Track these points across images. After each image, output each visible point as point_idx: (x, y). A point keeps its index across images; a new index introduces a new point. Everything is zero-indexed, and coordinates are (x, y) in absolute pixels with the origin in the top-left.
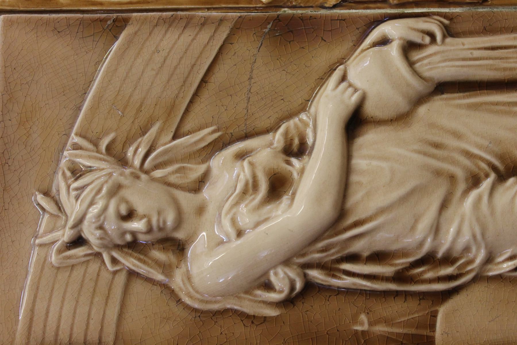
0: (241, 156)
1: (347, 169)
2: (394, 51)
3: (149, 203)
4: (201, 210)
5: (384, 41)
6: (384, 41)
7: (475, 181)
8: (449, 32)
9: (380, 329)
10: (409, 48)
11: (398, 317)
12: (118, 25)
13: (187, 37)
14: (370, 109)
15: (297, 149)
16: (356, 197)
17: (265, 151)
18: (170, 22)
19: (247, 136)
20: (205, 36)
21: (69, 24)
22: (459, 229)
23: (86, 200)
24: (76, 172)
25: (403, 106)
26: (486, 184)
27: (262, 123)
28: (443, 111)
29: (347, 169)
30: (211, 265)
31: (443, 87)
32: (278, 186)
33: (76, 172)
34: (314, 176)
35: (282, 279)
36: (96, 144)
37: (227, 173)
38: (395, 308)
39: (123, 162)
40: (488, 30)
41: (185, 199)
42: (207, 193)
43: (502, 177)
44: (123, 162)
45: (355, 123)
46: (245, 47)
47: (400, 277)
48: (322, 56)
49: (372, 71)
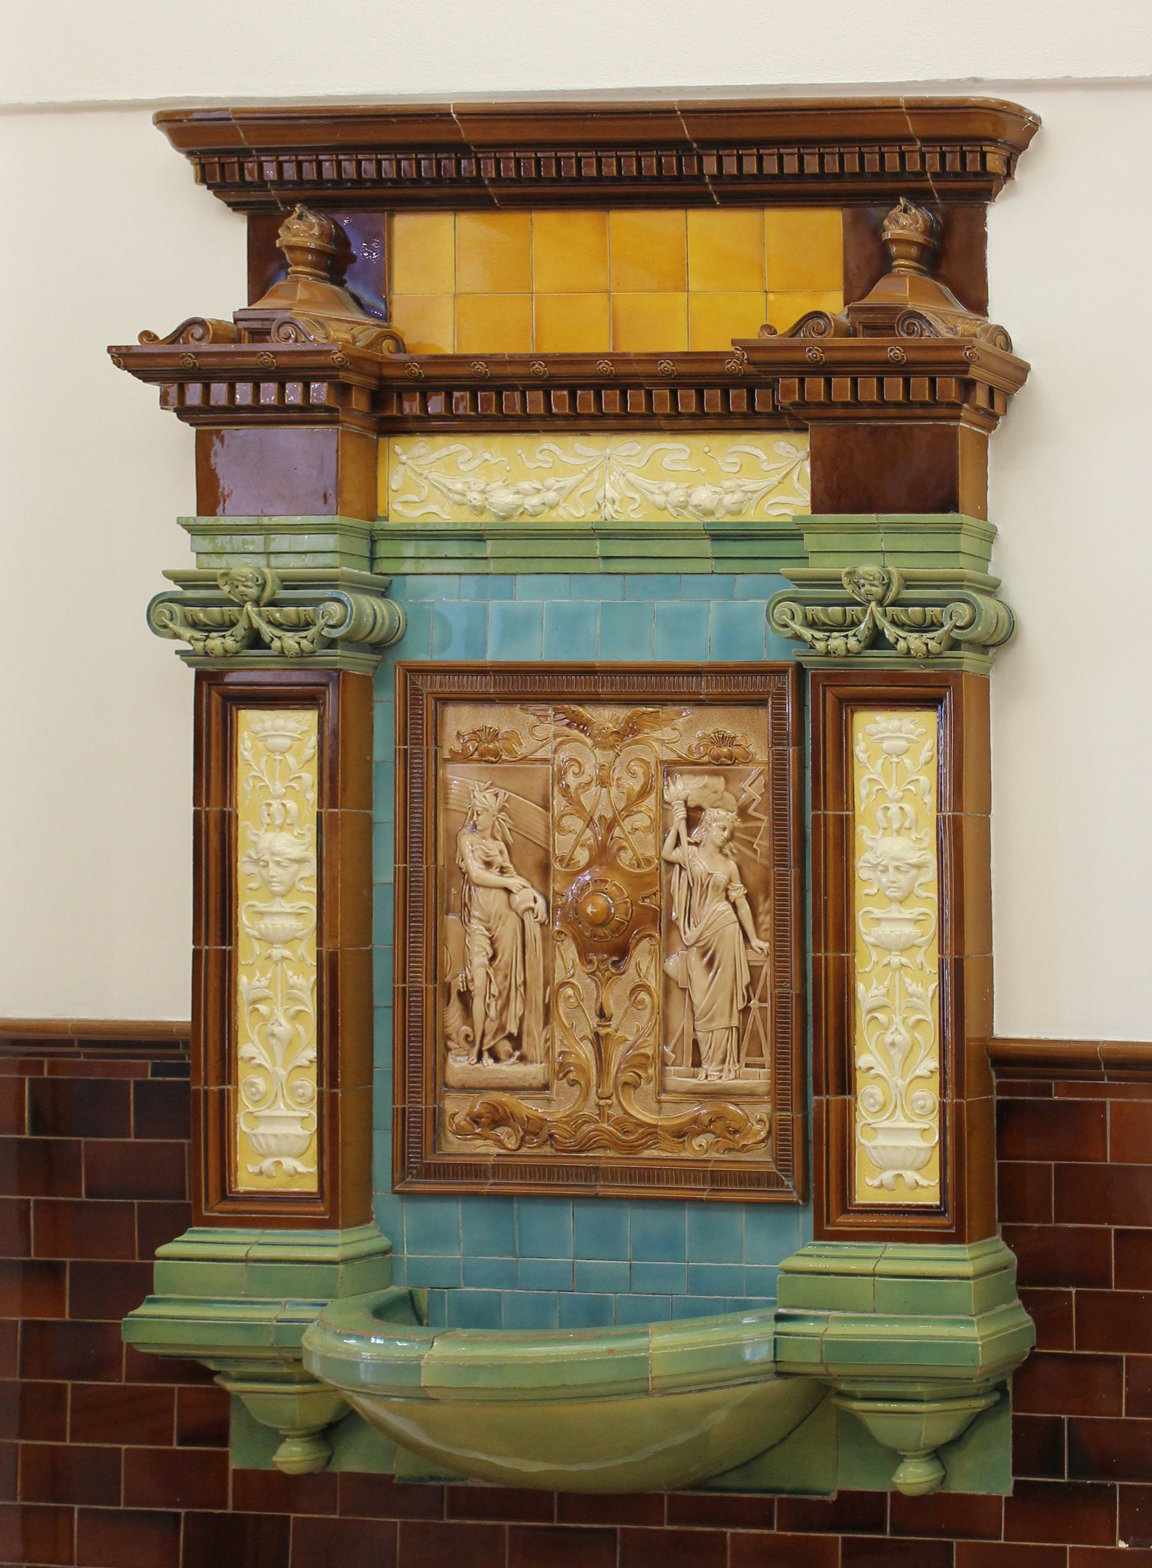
0: (501, 852)
1: (492, 888)
2: (532, 904)
3: (483, 821)
4: (484, 838)
5: (535, 901)
6: (535, 901)
7: (488, 930)
8: (542, 925)
9: (452, 898)
10: (533, 910)
11: (455, 903)
12: (546, 808)
13: (543, 833)
14: (512, 896)
15: (502, 871)
16: (481, 890)
17: (503, 860)
18: (548, 827)
19: (509, 853)
20: (543, 838)
21: (547, 791)
22: (475, 925)
23: (485, 800)
24: (496, 795)
25: (514, 906)
26: (487, 933)
27: (515, 860)
28: (513, 921)
29: (492, 888)
30: (467, 842)
31: (523, 921)
32: (488, 865)
33: (496, 795)
34: (493, 877)
35: (462, 865)
36: (507, 801)
37: (495, 848)
38: (459, 903)
39: (500, 811)
40: (545, 939)
41: (488, 832)
42: (490, 840)
43: (490, 939)
44: (500, 811)
45: (508, 891)
46: (540, 854)
47: (465, 905)
48: (536, 879)
49: (527, 895)
